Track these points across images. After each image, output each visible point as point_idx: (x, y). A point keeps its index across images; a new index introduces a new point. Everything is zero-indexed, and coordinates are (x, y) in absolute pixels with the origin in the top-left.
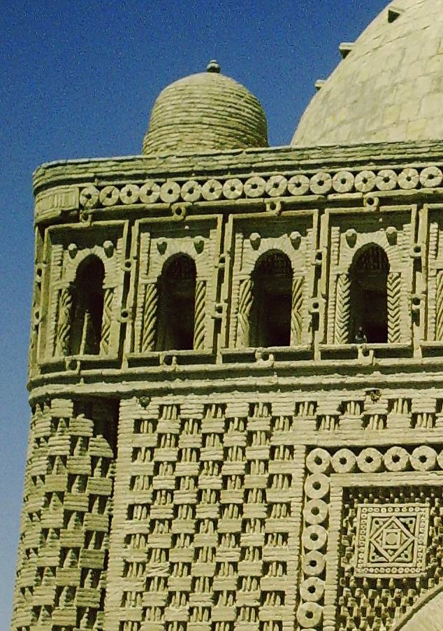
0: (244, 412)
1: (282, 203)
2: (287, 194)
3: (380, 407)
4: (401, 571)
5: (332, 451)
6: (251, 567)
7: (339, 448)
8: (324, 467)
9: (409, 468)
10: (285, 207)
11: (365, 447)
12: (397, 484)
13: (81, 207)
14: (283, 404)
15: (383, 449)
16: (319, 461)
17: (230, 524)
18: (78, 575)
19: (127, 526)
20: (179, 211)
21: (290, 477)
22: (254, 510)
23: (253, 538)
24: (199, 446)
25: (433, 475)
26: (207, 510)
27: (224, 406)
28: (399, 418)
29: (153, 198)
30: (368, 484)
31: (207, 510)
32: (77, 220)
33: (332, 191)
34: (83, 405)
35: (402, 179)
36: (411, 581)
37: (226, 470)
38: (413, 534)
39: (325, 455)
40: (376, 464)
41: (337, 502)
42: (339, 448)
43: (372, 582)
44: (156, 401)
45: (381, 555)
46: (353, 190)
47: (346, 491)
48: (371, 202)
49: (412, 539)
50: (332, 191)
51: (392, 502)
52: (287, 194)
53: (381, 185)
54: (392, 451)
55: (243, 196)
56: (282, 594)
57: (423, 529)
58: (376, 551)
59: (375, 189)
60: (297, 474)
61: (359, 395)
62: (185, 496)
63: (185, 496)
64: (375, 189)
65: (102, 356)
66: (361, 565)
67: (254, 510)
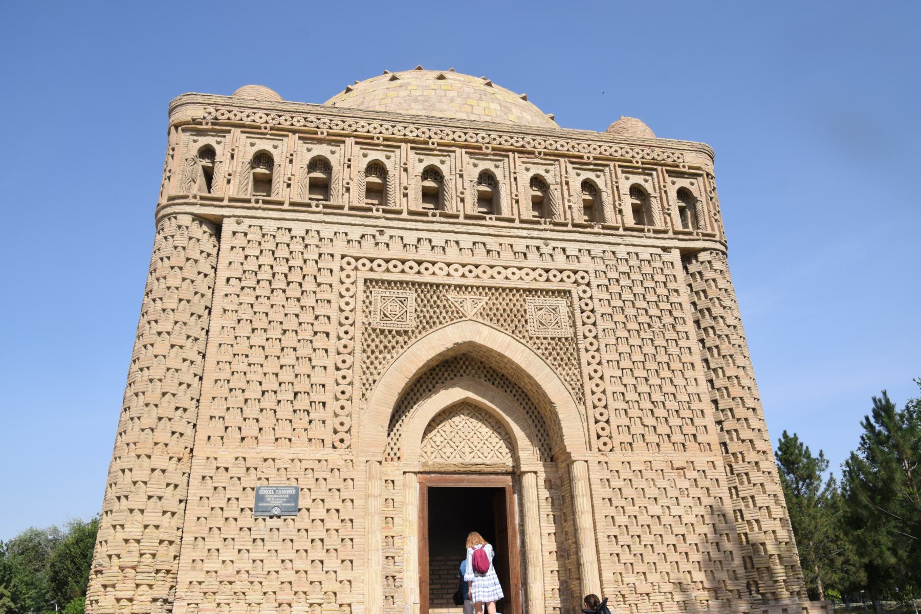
0: (303, 234)
1: (327, 132)
2: (330, 128)
3: (385, 238)
4: (400, 326)
5: (357, 259)
6: (307, 317)
7: (361, 258)
8: (352, 267)
9: (403, 271)
10: (329, 134)
11: (377, 259)
12: (397, 279)
13: (204, 118)
14: (327, 231)
16: (349, 263)
17: (294, 291)
19: (225, 289)
20: (266, 128)
21: (331, 271)
22: (309, 285)
23: (308, 301)
24: (274, 249)
25: (417, 276)
26: (279, 283)
27: (290, 230)
28: (396, 245)
29: (250, 119)
30: (379, 278)
31: (279, 283)
32: (201, 124)
33: (356, 131)
34: (201, 219)
35: (395, 130)
36: (406, 332)
37: (291, 263)
38: (406, 307)
39: (352, 261)
41: (361, 286)
42: (361, 258)
43: (382, 332)
44: (247, 222)
45: (387, 317)
46: (368, 132)
47: (366, 281)
49: (405, 309)
50: (356, 131)
51: (392, 289)
52: (330, 128)
53: (384, 131)
54: (393, 262)
55: (305, 126)
56: (328, 334)
57: (412, 304)
58: (384, 314)
60: (336, 269)
61: (373, 231)
62: (265, 274)
63: (265, 274)
64: (381, 133)
65: (213, 195)
66: (377, 322)
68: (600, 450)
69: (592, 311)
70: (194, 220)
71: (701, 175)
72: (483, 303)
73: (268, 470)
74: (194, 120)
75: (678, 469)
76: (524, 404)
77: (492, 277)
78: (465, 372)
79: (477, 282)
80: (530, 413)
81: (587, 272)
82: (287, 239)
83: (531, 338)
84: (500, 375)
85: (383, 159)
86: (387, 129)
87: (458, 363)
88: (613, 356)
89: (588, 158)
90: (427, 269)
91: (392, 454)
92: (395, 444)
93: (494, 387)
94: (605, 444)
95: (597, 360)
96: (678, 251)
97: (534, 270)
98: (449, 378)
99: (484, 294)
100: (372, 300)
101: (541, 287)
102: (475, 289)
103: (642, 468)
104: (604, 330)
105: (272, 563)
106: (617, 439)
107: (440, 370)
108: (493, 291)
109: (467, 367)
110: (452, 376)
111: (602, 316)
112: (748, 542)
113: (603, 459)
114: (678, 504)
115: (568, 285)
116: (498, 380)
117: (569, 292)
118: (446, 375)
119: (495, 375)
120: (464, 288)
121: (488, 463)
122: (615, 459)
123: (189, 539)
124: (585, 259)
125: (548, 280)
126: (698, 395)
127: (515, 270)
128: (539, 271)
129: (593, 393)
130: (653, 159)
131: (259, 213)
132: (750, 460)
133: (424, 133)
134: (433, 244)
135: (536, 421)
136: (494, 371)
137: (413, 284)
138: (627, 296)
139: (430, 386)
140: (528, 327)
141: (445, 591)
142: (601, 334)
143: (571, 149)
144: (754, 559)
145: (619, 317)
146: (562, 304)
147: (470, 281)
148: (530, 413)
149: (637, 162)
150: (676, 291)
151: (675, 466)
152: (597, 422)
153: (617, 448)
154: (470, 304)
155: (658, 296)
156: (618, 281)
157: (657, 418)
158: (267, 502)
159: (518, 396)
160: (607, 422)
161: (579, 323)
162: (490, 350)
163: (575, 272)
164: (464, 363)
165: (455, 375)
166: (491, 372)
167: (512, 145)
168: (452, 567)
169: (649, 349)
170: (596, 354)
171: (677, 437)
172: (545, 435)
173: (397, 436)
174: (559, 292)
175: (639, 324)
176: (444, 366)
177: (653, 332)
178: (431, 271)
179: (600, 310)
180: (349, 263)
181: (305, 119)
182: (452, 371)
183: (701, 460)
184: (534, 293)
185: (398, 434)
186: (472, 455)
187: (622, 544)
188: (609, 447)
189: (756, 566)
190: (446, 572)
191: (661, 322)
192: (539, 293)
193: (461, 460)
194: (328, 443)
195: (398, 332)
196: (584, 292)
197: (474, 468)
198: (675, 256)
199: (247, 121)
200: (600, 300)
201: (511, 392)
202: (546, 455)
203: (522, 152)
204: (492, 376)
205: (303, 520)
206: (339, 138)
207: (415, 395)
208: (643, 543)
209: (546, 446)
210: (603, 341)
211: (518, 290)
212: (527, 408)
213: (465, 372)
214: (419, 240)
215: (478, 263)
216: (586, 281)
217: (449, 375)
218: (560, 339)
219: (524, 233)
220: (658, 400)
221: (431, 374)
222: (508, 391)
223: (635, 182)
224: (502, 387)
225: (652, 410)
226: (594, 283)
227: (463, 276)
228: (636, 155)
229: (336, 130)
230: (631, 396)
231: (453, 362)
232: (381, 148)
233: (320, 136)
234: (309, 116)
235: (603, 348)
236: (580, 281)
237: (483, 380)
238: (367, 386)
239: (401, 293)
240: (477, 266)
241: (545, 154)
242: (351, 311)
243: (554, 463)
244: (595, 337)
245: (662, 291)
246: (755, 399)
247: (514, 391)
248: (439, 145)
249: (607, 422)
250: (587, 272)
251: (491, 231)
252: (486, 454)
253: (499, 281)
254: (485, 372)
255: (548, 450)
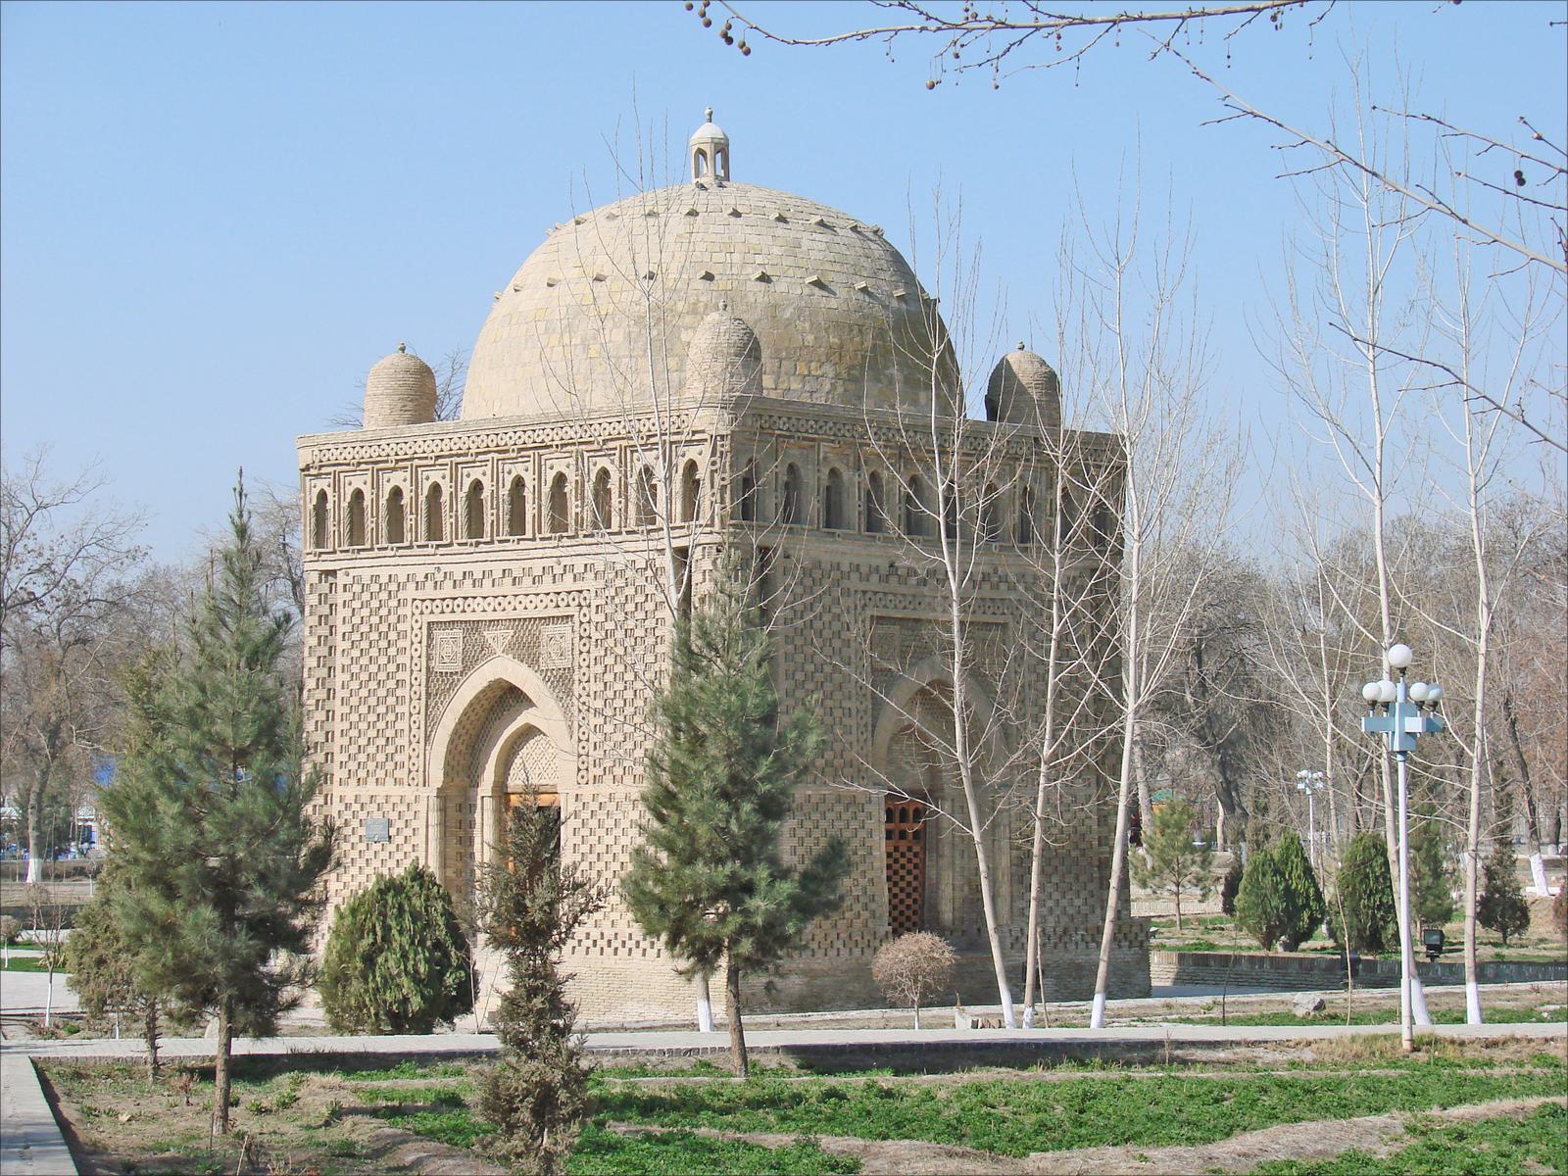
44: (352, 572)
60: (409, 614)
115: (573, 610)
194: (405, 781)
219: (540, 553)
241: (563, 445)
251: (513, 555)
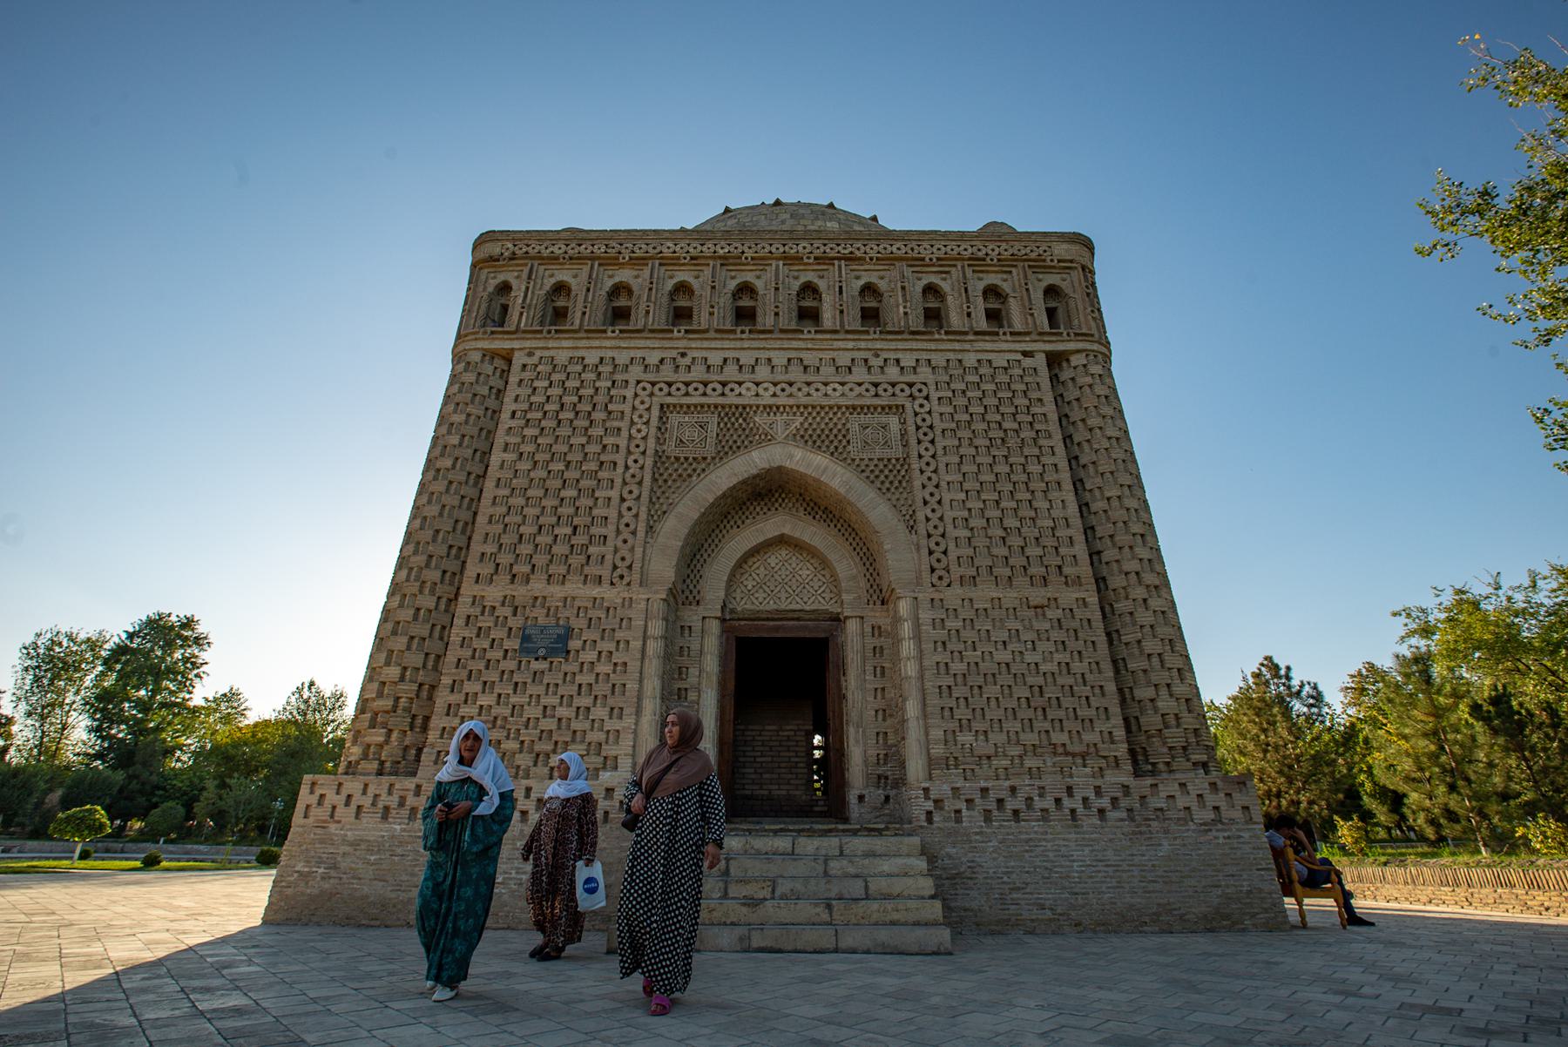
2: (633, 252)
7: (659, 382)
8: (647, 392)
9: (705, 394)
13: (502, 254)
15: (687, 384)
16: (644, 389)
18: (470, 451)
23: (597, 431)
25: (721, 398)
27: (583, 359)
31: (567, 415)
32: (498, 260)
33: (661, 252)
36: (705, 459)
40: (683, 391)
41: (655, 412)
42: (659, 382)
43: (677, 459)
44: (538, 354)
46: (675, 252)
48: (685, 258)
50: (661, 252)
52: (633, 252)
53: (691, 250)
54: (694, 385)
55: (606, 252)
57: (713, 428)
59: (688, 252)
66: (671, 449)
67: (599, 415)
68: (933, 586)
69: (931, 427)
70: (484, 355)
71: (1076, 268)
72: (798, 424)
73: (539, 613)
74: (491, 257)
75: (1036, 607)
76: (851, 540)
77: (809, 395)
78: (780, 505)
79: (791, 401)
80: (858, 549)
81: (925, 384)
82: (579, 368)
83: (853, 460)
84: (822, 508)
85: (691, 280)
86: (695, 248)
87: (773, 496)
88: (955, 477)
89: (931, 259)
90: (732, 390)
91: (691, 598)
92: (695, 586)
93: (815, 522)
94: (940, 578)
95: (934, 482)
96: (1043, 355)
97: (860, 384)
98: (761, 513)
99: (798, 414)
100: (668, 426)
101: (868, 403)
102: (787, 409)
103: (988, 606)
104: (945, 447)
105: (533, 712)
106: (956, 571)
107: (752, 504)
108: (810, 409)
109: (783, 500)
110: (765, 510)
111: (943, 432)
112: (1133, 699)
113: (937, 596)
114: (1034, 649)
116: (820, 513)
117: (903, 406)
118: (758, 509)
119: (816, 509)
120: (775, 409)
121: (808, 608)
122: (953, 596)
123: (446, 682)
124: (924, 371)
125: (876, 395)
126: (1066, 519)
127: (837, 386)
128: (866, 386)
129: (928, 519)
130: (1012, 255)
131: (551, 344)
132: (1135, 597)
133: (736, 248)
134: (741, 363)
135: (865, 559)
136: (815, 504)
137: (716, 407)
138: (976, 409)
139: (739, 522)
140: (850, 448)
141: (777, 765)
142: (940, 452)
143: (910, 252)
144: (1141, 720)
145: (965, 434)
146: (893, 422)
147: (781, 401)
148: (858, 549)
149: (992, 260)
150: (1040, 400)
151: (1031, 604)
152: (931, 553)
153: (956, 585)
154: (780, 425)
155: (1016, 407)
156: (964, 392)
157: (1009, 547)
158: (535, 643)
159: (843, 531)
160: (945, 553)
161: (913, 441)
162: (803, 475)
163: (911, 385)
164: (780, 496)
165: (769, 509)
166: (812, 504)
167: (839, 252)
168: (785, 738)
169: (1002, 468)
170: (933, 476)
171: (1037, 570)
172: (875, 574)
173: (698, 576)
174: (890, 407)
175: (990, 439)
176: (756, 500)
177: (1008, 448)
178: (737, 392)
179: (939, 426)
180: (644, 389)
181: (606, 245)
182: (766, 504)
183: (1069, 596)
184: (859, 410)
185: (698, 576)
186: (789, 600)
187: (958, 695)
188: (946, 581)
189: (1143, 729)
190: (778, 743)
191: (1019, 437)
192: (866, 411)
193: (775, 607)
194: (606, 580)
195: (694, 459)
196: (921, 406)
197: (790, 615)
198: (1040, 361)
199: (546, 253)
200: (941, 414)
201: (835, 526)
202: (875, 597)
203: (850, 259)
204: (813, 509)
205: (572, 667)
206: (642, 262)
207: (721, 531)
208: (985, 696)
209: (875, 587)
210: (943, 460)
211: (839, 407)
212: (854, 544)
213: (780, 505)
214: (725, 360)
215: (793, 380)
216: (925, 393)
217: (762, 509)
218: (889, 460)
220: (1013, 526)
221: (741, 509)
222: (832, 525)
223: (990, 282)
224: (825, 521)
225: (1004, 538)
226: (934, 396)
227: (774, 395)
228: (990, 252)
229: (639, 254)
230: (977, 522)
231: (767, 495)
232: (689, 268)
233: (621, 261)
234: (611, 242)
235: (942, 467)
236: (917, 394)
237: (801, 514)
238: (655, 518)
239: (703, 417)
240: (791, 384)
241: (878, 259)
242: (643, 438)
243: (885, 607)
244: (933, 456)
245: (1021, 401)
246: (1144, 523)
247: (839, 526)
248: (752, 258)
249: (945, 553)
250: (925, 384)
252: (805, 599)
253: (817, 398)
254: (805, 505)
255: (878, 591)
